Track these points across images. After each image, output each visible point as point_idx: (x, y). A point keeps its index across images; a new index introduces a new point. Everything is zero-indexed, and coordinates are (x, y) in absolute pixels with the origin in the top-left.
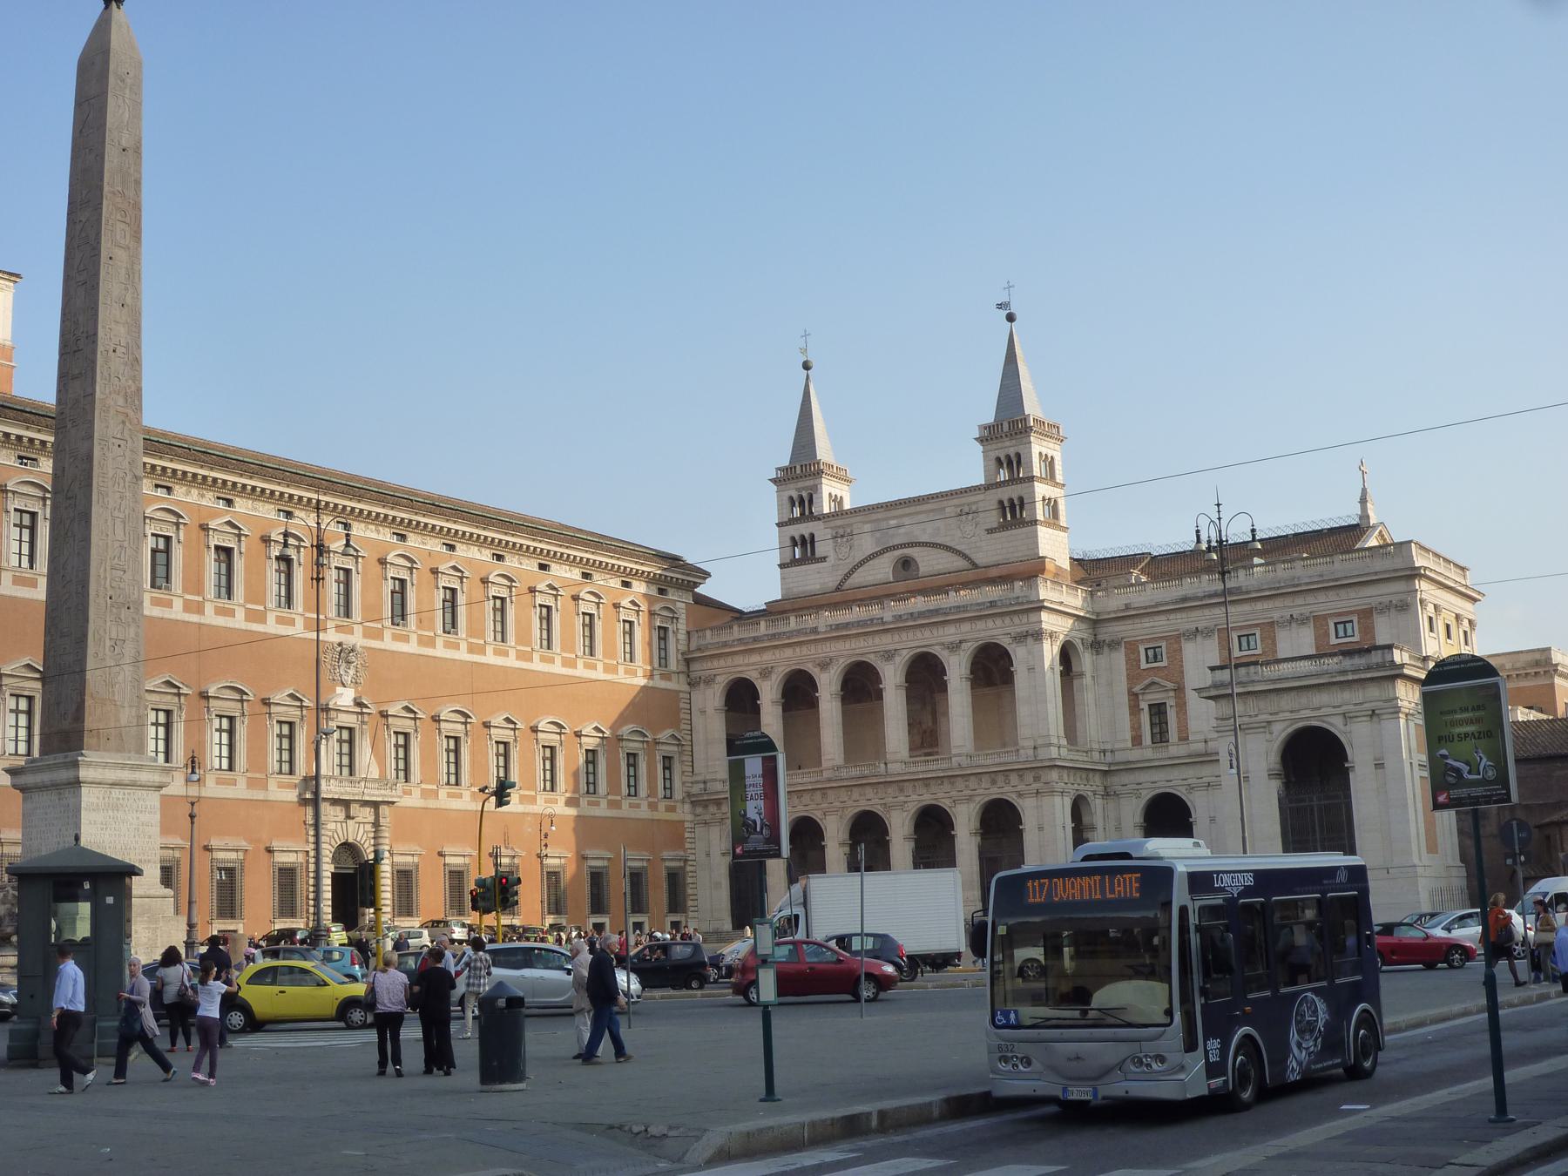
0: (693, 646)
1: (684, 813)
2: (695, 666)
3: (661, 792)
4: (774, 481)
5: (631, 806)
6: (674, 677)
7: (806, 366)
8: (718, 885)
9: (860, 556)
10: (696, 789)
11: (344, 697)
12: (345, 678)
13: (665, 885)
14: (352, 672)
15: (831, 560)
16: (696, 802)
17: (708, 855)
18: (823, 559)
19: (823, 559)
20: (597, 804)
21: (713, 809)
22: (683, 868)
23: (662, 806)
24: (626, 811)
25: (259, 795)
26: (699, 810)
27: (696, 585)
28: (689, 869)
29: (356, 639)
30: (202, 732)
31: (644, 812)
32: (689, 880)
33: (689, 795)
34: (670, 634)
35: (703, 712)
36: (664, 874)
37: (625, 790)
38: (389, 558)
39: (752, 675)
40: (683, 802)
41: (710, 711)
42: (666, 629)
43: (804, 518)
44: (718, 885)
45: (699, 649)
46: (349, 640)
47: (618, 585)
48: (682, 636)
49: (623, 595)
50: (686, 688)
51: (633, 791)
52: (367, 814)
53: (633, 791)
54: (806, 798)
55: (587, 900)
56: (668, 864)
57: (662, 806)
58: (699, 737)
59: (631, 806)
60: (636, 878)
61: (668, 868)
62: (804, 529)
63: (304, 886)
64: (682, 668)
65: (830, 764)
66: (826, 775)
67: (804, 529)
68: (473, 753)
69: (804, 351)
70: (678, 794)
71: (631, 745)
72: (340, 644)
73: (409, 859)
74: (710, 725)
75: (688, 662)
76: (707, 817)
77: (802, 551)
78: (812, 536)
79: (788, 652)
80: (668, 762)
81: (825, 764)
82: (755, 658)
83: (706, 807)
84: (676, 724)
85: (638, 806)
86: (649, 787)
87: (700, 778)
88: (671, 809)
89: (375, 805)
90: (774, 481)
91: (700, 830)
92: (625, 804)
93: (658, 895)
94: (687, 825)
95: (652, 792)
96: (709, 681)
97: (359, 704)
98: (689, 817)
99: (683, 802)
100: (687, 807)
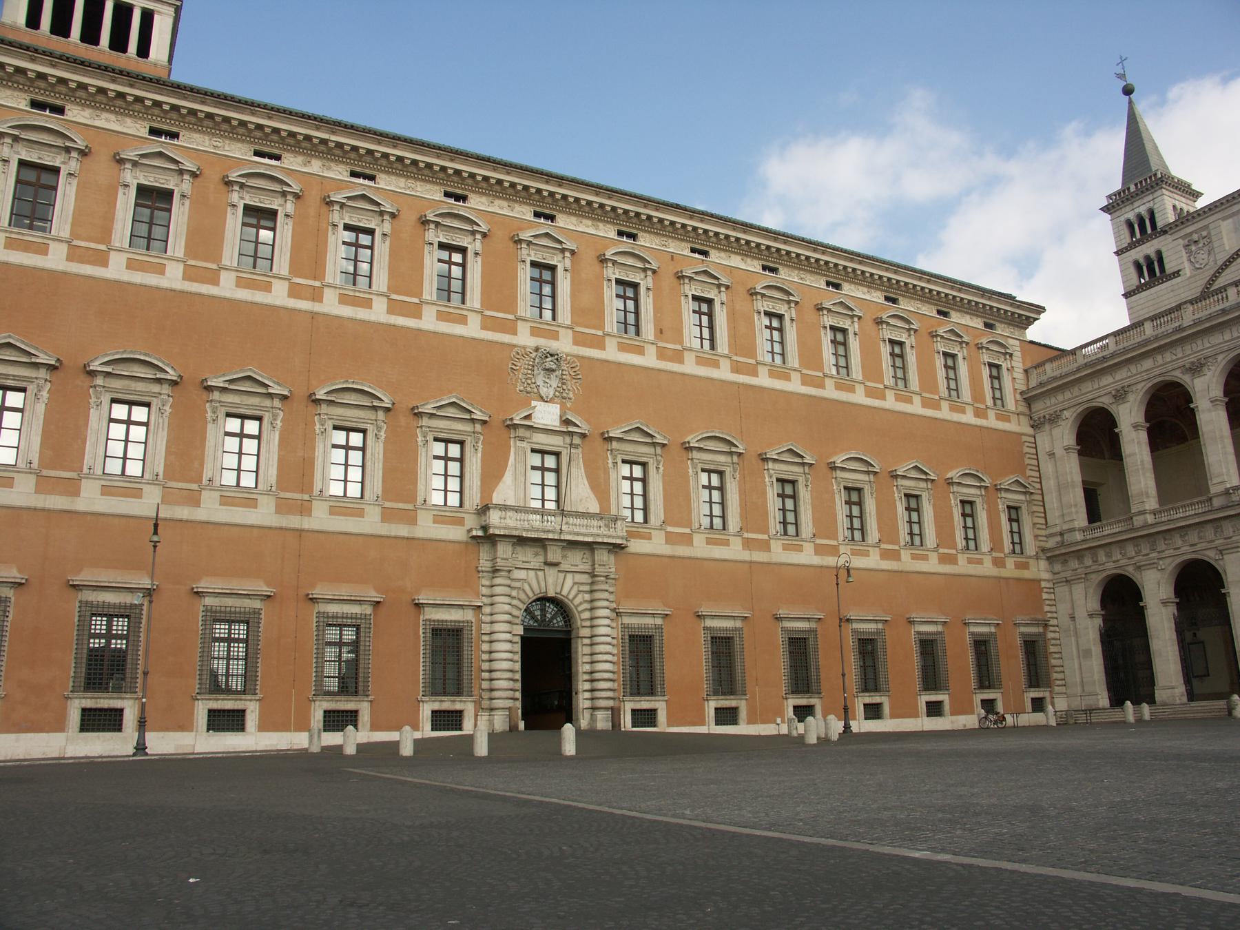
0: (1033, 383)
1: (1040, 570)
2: (1037, 406)
3: (1007, 547)
4: (1106, 209)
5: (970, 561)
6: (1014, 418)
7: (1128, 91)
8: (1087, 653)
9: (1222, 258)
10: (1051, 543)
11: (547, 415)
12: (543, 391)
13: (1021, 655)
14: (554, 382)
15: (1187, 270)
16: (1051, 557)
17: (1073, 618)
18: (1177, 274)
19: (1177, 274)
20: (925, 558)
21: (1074, 564)
22: (1044, 634)
23: (1010, 563)
24: (963, 566)
25: (402, 530)
26: (1058, 567)
27: (1029, 321)
28: (1050, 635)
29: (564, 345)
30: (309, 442)
31: (987, 568)
32: (1052, 649)
33: (1043, 550)
34: (1004, 372)
35: (1052, 455)
36: (1019, 641)
37: (960, 543)
38: (608, 255)
39: (1105, 401)
40: (1037, 557)
41: (1059, 452)
42: (998, 367)
43: (1145, 238)
44: (1087, 653)
45: (1041, 385)
46: (553, 345)
47: (934, 314)
48: (1019, 374)
49: (940, 325)
50: (1031, 431)
51: (972, 541)
52: (576, 560)
53: (972, 541)
54: (1193, 537)
55: (916, 674)
56: (1023, 629)
57: (1010, 563)
58: (1050, 484)
59: (970, 561)
60: (982, 647)
61: (1022, 634)
62: (1149, 249)
63: (476, 653)
64: (1022, 408)
65: (1221, 488)
66: (1217, 503)
67: (1149, 249)
68: (743, 493)
69: (1122, 76)
70: (1031, 547)
71: (965, 490)
72: (537, 349)
73: (649, 621)
74: (1062, 469)
75: (1029, 401)
76: (1068, 574)
77: (1151, 272)
78: (1159, 254)
79: (1147, 364)
80: (1014, 512)
81: (1214, 490)
82: (1107, 380)
83: (1065, 562)
84: (1022, 468)
85: (980, 562)
86: (992, 539)
87: (1058, 529)
88: (1019, 566)
89: (590, 546)
90: (1106, 209)
91: (1062, 590)
92: (962, 559)
93: (1012, 665)
94: (1043, 584)
95: (996, 545)
96: (1054, 419)
97: (567, 422)
98: (1045, 576)
99: (1037, 557)
100: (1043, 564)
